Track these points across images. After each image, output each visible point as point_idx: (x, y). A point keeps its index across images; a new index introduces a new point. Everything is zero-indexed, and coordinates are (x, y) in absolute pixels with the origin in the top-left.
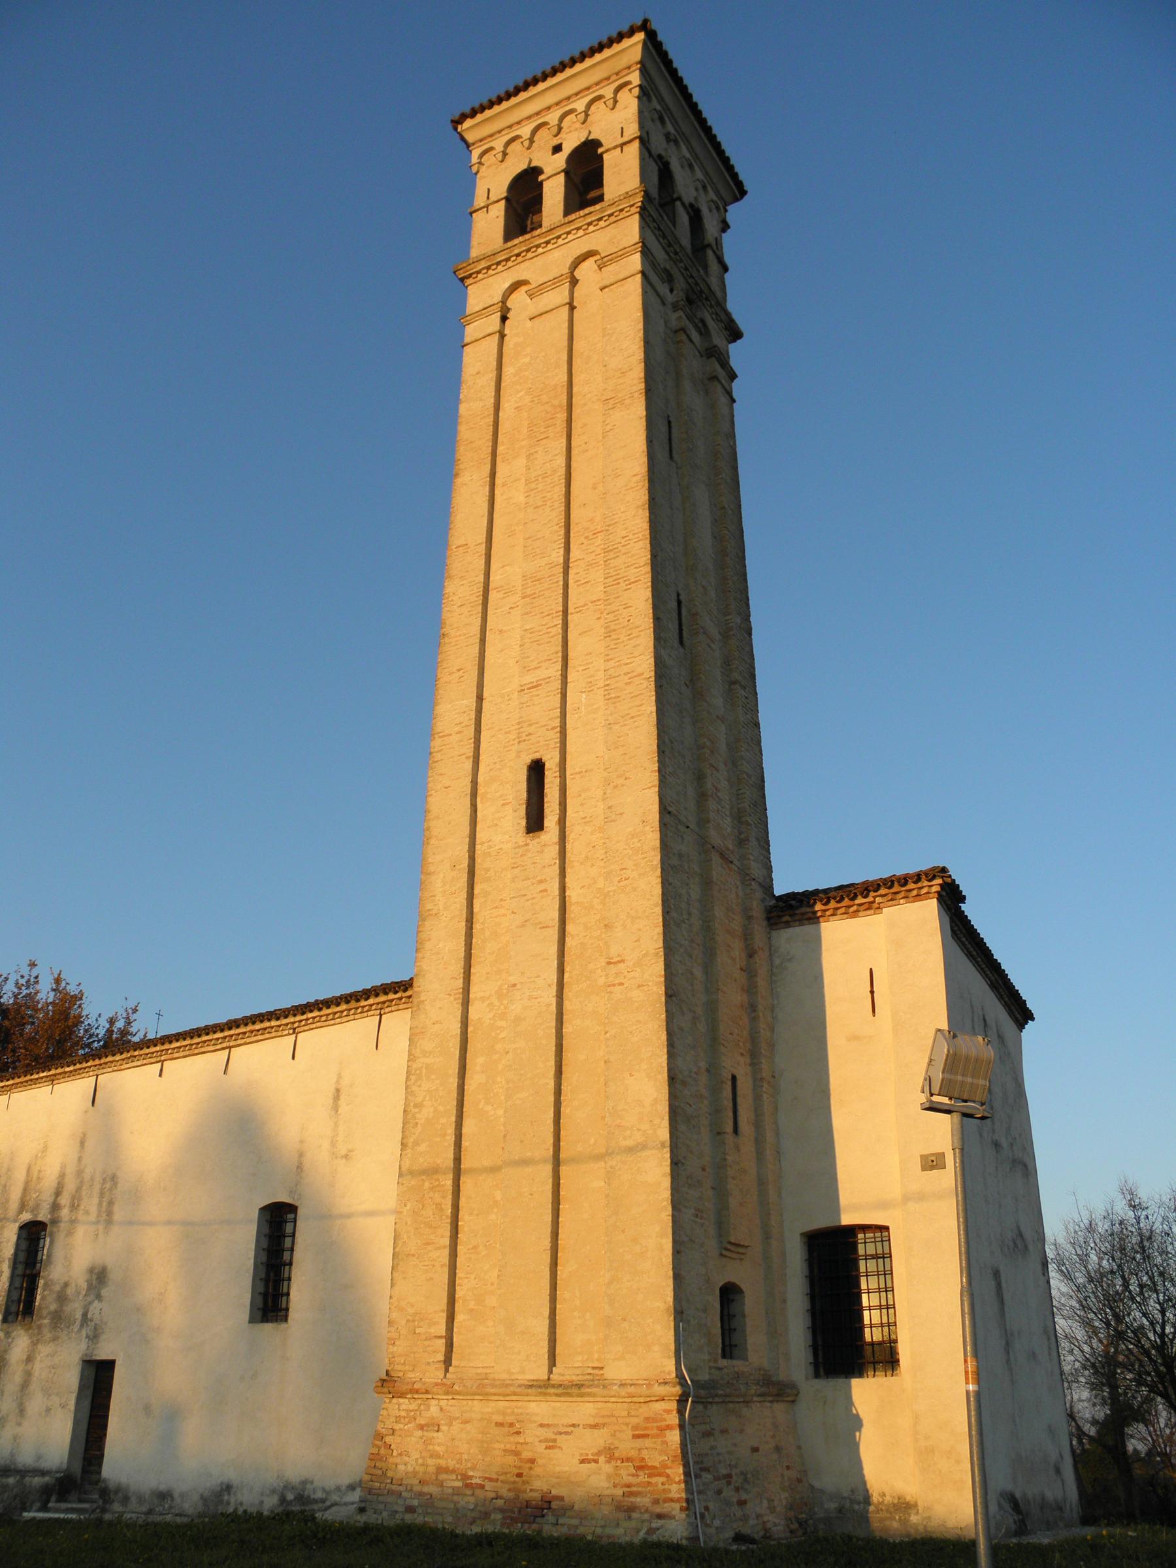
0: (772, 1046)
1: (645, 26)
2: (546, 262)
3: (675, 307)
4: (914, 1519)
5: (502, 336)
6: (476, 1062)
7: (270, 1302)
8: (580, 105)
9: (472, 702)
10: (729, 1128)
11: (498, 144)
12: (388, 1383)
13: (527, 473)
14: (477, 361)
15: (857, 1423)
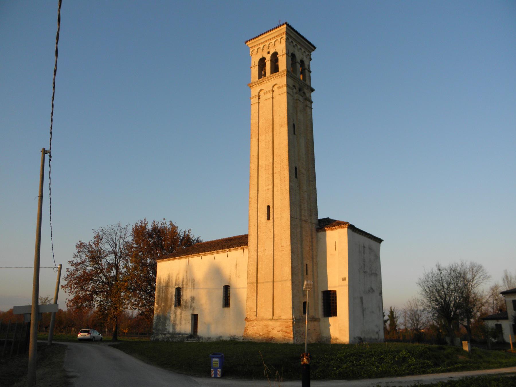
0: (317, 256)
1: (286, 23)
2: (267, 85)
3: (296, 93)
4: (338, 341)
5: (259, 103)
6: (260, 263)
7: (226, 303)
8: (273, 41)
9: (256, 191)
10: (305, 273)
11: (256, 49)
12: (247, 319)
13: (265, 138)
14: (254, 109)
15: (330, 325)
